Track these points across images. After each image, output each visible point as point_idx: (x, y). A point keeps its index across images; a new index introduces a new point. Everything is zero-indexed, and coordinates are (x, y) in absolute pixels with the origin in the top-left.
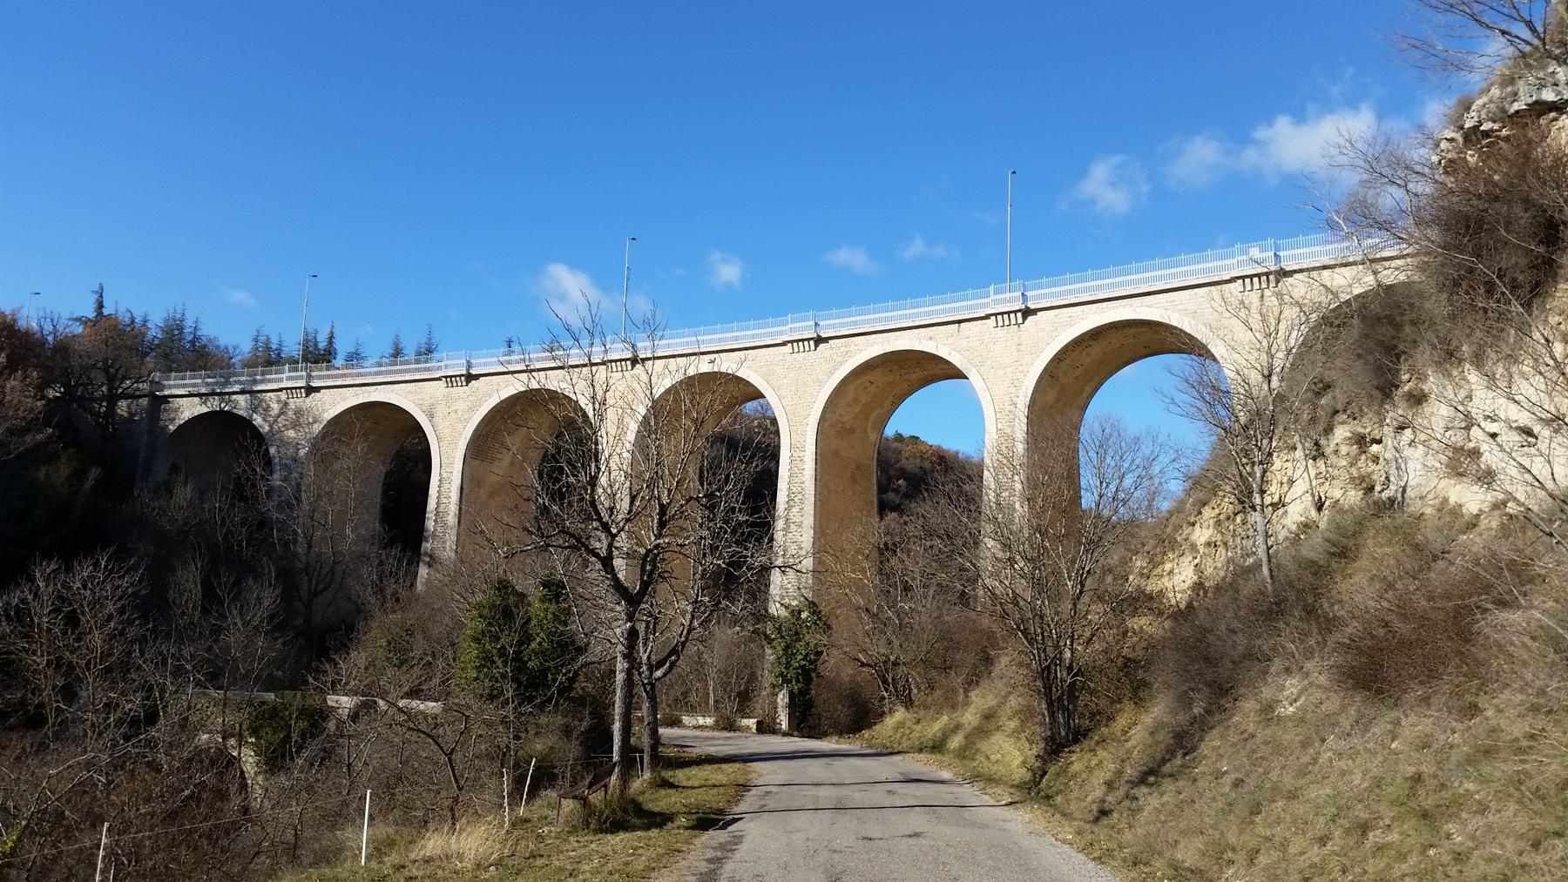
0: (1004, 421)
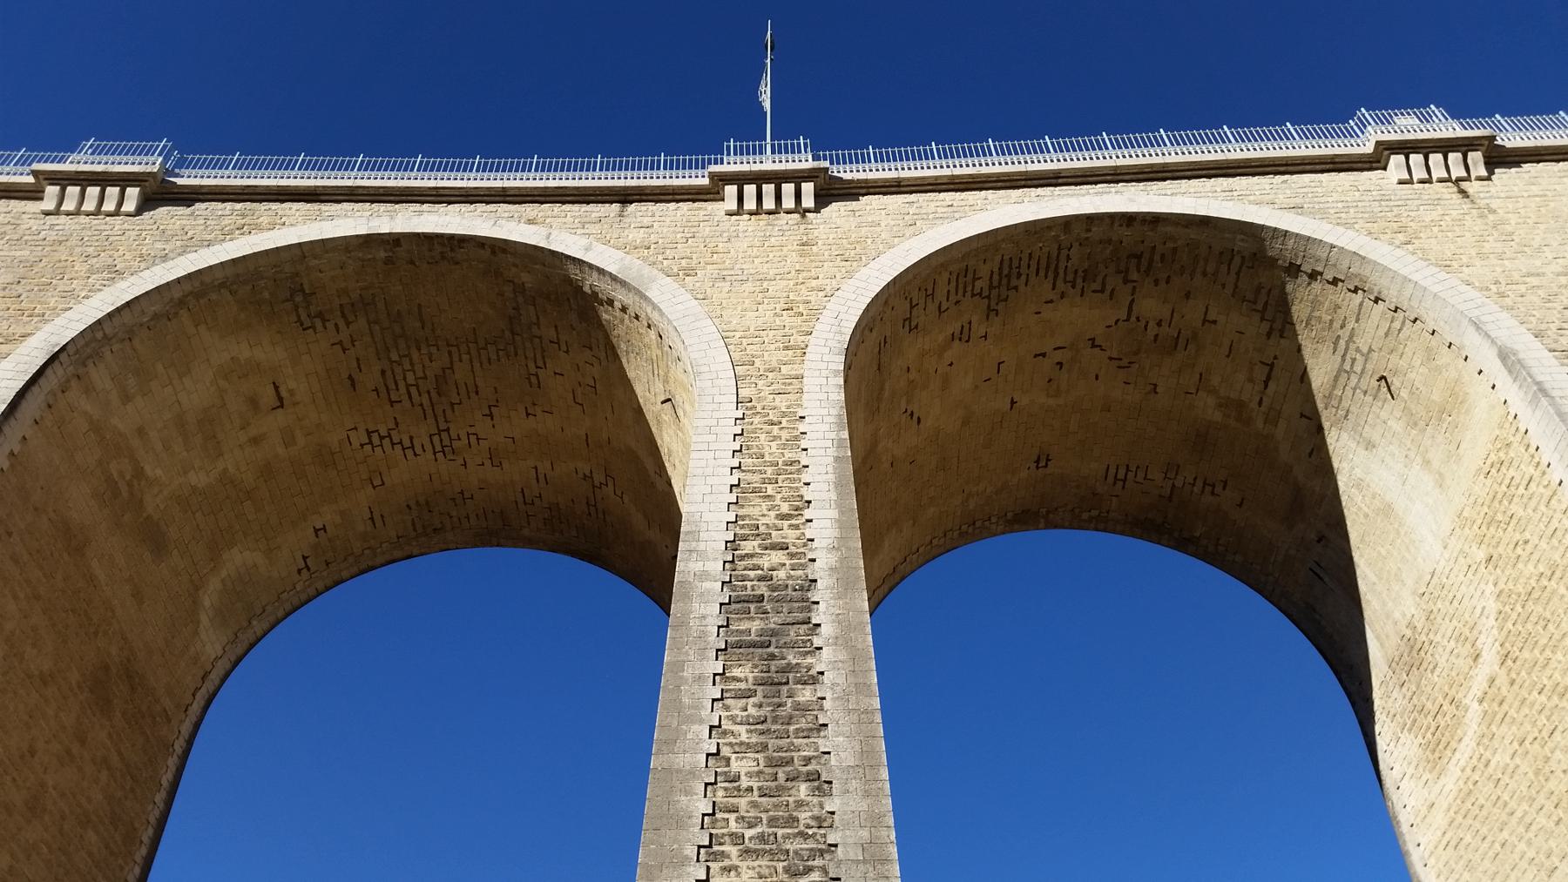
0: (761, 383)
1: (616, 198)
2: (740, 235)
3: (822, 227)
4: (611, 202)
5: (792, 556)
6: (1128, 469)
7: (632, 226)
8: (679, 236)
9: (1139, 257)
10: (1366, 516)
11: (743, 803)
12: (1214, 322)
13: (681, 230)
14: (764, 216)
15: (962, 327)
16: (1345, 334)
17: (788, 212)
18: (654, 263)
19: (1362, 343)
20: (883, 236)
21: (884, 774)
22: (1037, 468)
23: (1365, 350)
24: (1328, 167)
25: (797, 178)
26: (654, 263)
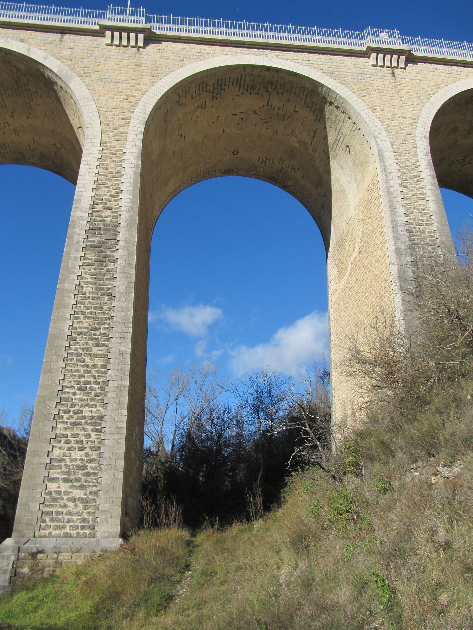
0: (111, 134)
1: (59, 31)
2: (111, 57)
3: (145, 56)
4: (57, 33)
5: (113, 212)
6: (266, 159)
7: (66, 47)
8: (85, 55)
9: (272, 83)
10: (338, 191)
11: (86, 301)
12: (298, 112)
13: (86, 51)
14: (122, 48)
15: (202, 103)
16: (339, 126)
17: (132, 47)
18: (73, 69)
19: (344, 131)
20: (170, 65)
21: (133, 295)
22: (234, 154)
23: (344, 135)
24: (348, 54)
25: (137, 31)
26: (73, 69)
